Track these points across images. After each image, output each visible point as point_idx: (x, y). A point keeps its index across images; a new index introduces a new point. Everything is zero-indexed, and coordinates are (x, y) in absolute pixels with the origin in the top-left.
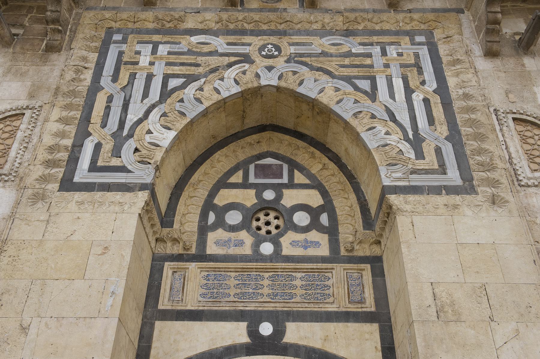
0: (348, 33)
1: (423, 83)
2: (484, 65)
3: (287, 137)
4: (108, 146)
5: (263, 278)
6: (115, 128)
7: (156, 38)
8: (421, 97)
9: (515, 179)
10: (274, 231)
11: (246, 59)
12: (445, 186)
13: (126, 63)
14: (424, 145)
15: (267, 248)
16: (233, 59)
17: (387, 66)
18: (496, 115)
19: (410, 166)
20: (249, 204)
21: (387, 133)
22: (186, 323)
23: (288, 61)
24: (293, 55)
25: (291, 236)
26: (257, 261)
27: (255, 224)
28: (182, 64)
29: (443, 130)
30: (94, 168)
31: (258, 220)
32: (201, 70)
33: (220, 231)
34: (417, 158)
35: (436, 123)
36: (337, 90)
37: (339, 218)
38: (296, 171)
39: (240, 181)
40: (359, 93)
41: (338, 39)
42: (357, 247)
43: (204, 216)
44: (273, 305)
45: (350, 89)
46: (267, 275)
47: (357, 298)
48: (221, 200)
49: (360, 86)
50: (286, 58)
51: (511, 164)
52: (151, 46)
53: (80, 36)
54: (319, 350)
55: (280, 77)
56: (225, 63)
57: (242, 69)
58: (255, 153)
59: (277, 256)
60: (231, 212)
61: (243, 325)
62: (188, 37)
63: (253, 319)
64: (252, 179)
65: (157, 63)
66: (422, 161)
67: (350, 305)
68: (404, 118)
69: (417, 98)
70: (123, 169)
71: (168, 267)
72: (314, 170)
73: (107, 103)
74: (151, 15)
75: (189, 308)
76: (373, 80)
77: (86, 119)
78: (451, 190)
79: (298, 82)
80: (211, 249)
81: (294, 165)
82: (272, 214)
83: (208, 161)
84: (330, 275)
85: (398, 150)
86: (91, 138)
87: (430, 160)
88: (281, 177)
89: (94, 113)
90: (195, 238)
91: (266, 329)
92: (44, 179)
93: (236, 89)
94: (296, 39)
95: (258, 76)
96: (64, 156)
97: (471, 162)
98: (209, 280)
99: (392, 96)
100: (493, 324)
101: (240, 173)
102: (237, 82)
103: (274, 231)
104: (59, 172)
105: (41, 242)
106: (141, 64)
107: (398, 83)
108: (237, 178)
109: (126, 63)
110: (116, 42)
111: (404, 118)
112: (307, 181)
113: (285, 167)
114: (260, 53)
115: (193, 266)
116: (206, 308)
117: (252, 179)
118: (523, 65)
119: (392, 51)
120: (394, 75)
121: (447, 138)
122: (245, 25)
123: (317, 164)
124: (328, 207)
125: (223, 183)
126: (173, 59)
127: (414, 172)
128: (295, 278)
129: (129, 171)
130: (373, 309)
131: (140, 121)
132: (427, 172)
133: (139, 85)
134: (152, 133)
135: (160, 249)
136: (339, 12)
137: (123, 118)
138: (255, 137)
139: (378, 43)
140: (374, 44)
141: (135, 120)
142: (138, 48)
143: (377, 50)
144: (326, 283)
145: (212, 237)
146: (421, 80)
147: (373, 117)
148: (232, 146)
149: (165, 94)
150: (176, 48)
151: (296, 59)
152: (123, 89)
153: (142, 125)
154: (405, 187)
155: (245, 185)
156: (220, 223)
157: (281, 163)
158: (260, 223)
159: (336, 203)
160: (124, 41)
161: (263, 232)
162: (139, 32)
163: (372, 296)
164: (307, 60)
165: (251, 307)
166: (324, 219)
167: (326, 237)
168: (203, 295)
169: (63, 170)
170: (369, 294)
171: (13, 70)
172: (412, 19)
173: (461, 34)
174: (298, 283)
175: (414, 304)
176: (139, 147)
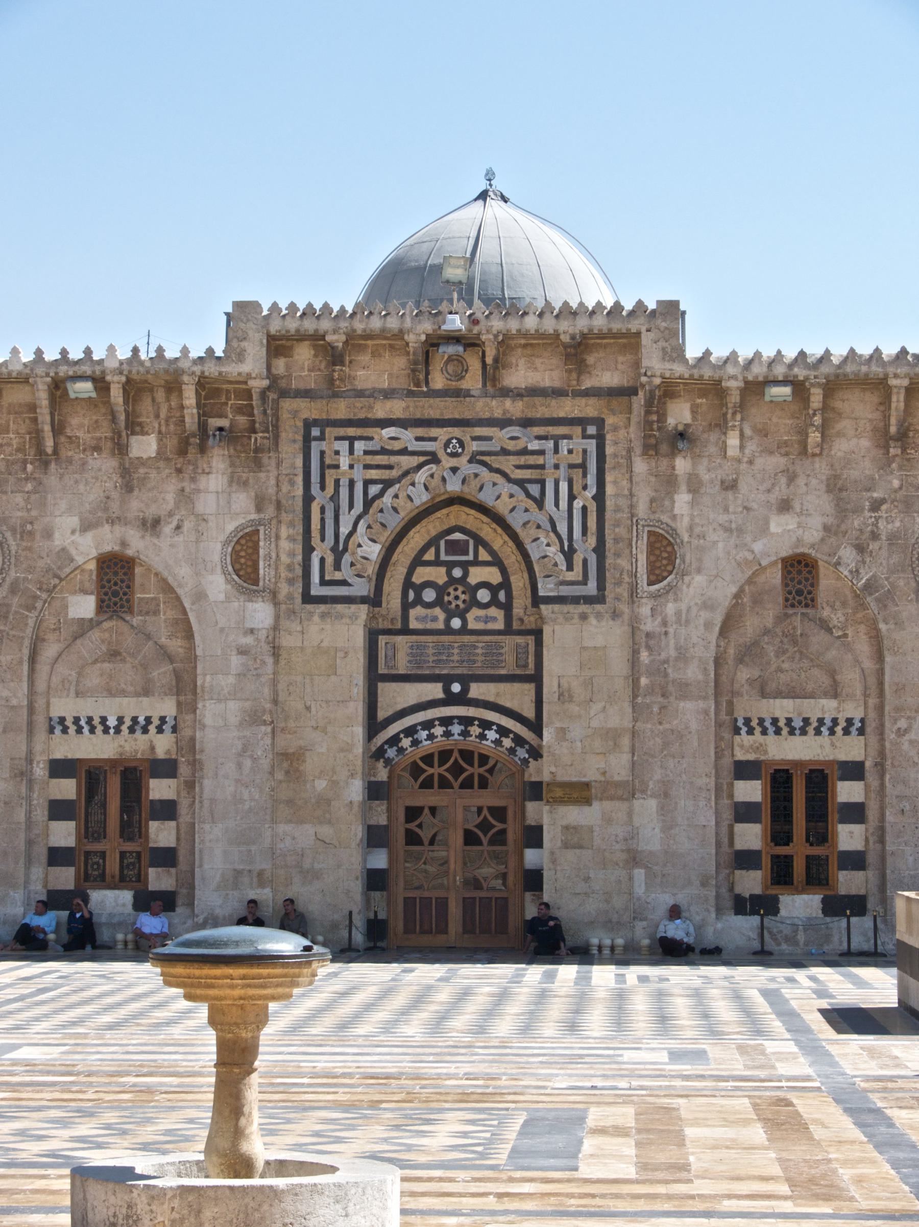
0: (526, 423)
1: (585, 487)
2: (640, 466)
3: (473, 512)
4: (330, 559)
5: (453, 648)
6: (332, 543)
7: (351, 431)
8: (581, 504)
10: (462, 606)
14: (575, 556)
15: (456, 623)
16: (422, 459)
17: (557, 467)
21: (548, 545)
23: (470, 461)
25: (475, 612)
28: (378, 467)
29: (592, 541)
30: (323, 582)
31: (449, 594)
32: (395, 473)
33: (419, 608)
36: (511, 496)
39: (433, 558)
41: (515, 431)
43: (405, 594)
45: (521, 495)
47: (522, 663)
48: (417, 579)
49: (532, 492)
52: (347, 443)
53: (283, 435)
55: (464, 481)
58: (445, 527)
59: (464, 630)
61: (439, 686)
62: (378, 429)
63: (447, 681)
64: (443, 557)
68: (562, 528)
69: (578, 504)
70: (344, 583)
71: (382, 640)
72: (497, 545)
76: (542, 483)
78: (589, 600)
81: (480, 541)
83: (405, 541)
86: (315, 553)
87: (576, 574)
88: (467, 554)
89: (313, 527)
90: (400, 613)
91: (456, 688)
94: (479, 431)
95: (444, 479)
96: (299, 571)
97: (608, 574)
99: (557, 505)
101: (433, 550)
102: (426, 488)
105: (302, 649)
107: (564, 487)
108: (429, 556)
110: (316, 439)
111: (562, 528)
112: (489, 558)
113: (471, 542)
115: (399, 639)
118: (673, 468)
119: (564, 445)
121: (594, 550)
123: (498, 540)
124: (506, 584)
126: (369, 459)
129: (350, 585)
143: (550, 444)
147: (539, 527)
149: (368, 503)
152: (331, 498)
154: (554, 597)
155: (437, 563)
156: (419, 601)
159: (513, 579)
160: (322, 438)
161: (453, 606)
164: (486, 459)
165: (445, 672)
166: (502, 596)
167: (502, 612)
168: (410, 662)
171: (235, 479)
173: (628, 426)
174: (479, 651)
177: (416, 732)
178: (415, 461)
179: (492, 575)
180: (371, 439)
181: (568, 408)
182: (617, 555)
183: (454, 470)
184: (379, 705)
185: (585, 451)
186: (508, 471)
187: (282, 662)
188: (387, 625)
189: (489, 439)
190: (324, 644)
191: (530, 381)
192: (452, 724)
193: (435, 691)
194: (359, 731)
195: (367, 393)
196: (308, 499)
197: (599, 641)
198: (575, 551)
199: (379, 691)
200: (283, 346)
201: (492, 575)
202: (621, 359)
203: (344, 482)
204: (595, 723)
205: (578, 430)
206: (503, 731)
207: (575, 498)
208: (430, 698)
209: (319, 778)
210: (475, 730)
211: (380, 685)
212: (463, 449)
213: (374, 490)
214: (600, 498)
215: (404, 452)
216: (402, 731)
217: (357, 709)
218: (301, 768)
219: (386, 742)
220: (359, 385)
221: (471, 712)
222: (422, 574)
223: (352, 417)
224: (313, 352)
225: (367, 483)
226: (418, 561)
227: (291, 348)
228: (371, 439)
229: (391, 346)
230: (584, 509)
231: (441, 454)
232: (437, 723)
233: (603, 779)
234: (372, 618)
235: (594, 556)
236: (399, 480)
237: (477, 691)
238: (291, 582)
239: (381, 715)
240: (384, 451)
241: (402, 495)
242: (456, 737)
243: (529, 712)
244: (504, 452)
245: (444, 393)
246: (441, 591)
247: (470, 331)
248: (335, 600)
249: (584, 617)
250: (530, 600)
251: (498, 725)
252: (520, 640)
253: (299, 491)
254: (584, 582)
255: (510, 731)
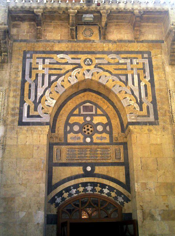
0: (118, 53)
1: (145, 77)
4: (32, 107)
7: (44, 55)
8: (144, 84)
9: (172, 120)
10: (90, 133)
11: (79, 66)
12: (149, 122)
13: (34, 69)
14: (143, 105)
15: (88, 140)
16: (74, 66)
18: (170, 92)
19: (138, 114)
20: (81, 123)
21: (131, 100)
22: (63, 167)
23: (95, 67)
24: (97, 64)
26: (85, 145)
27: (84, 130)
28: (55, 69)
29: (150, 99)
30: (28, 116)
31: (85, 128)
32: (62, 72)
33: (72, 133)
34: (140, 111)
35: (148, 95)
36: (113, 81)
37: (113, 127)
38: (98, 109)
40: (121, 83)
41: (114, 56)
42: (119, 139)
43: (65, 128)
44: (90, 160)
45: (118, 80)
46: (88, 150)
48: (71, 122)
50: (94, 66)
51: (172, 113)
52: (42, 60)
54: (106, 175)
55: (92, 75)
56: (71, 68)
57: (78, 71)
59: (92, 143)
60: (75, 126)
61: (81, 167)
62: (56, 55)
63: (85, 165)
64: (82, 112)
65: (45, 68)
66: (142, 112)
67: (116, 160)
68: (137, 93)
69: (142, 84)
70: (39, 116)
72: (105, 108)
73: (29, 87)
74: (40, 45)
75: (63, 162)
77: (22, 95)
78: (151, 123)
79: (99, 77)
80: (69, 141)
81: (97, 106)
82: (90, 126)
83: (66, 105)
84: (109, 149)
85: (134, 107)
86: (25, 104)
91: (89, 169)
92: (13, 121)
93: (76, 81)
94: (98, 56)
95: (84, 74)
96: (17, 111)
97: (159, 112)
98: (69, 152)
100: (158, 170)
101: (78, 110)
102: (76, 78)
103: (90, 133)
104: (17, 117)
106: (39, 69)
107: (136, 77)
109: (34, 69)
110: (28, 58)
111: (137, 93)
112: (102, 113)
113: (94, 107)
114: (84, 63)
115: (63, 147)
116: (69, 162)
117: (82, 112)
119: (135, 61)
120: (135, 74)
121: (151, 102)
122: (78, 49)
123: (106, 106)
124: (109, 123)
125: (71, 114)
127: (138, 116)
128: (98, 151)
130: (123, 161)
131: (42, 96)
132: (143, 116)
133: (40, 79)
134: (47, 101)
135: (51, 141)
136: (115, 42)
137: (36, 94)
138: (83, 94)
139: (129, 58)
140: (128, 58)
141: (40, 95)
142: (37, 61)
143: (129, 61)
144: (108, 152)
145: (69, 136)
146: (145, 75)
147: (126, 93)
148: (74, 98)
149: (50, 84)
150: (52, 61)
151: (98, 66)
152: (34, 81)
153: (43, 98)
154: (135, 122)
155: (79, 115)
156: (72, 131)
157: (92, 105)
158: (85, 130)
160: (31, 57)
162: (36, 52)
163: (123, 157)
165: (84, 161)
167: (108, 135)
169: (18, 117)
170: (122, 155)
172: (143, 46)
174: (99, 152)
175: (135, 165)
176: (43, 107)
177: (71, 190)
178: (71, 67)
179: (104, 120)
180: (53, 58)
181: (137, 47)
182: (163, 103)
183: (88, 71)
184: (53, 177)
185: (144, 64)
186: (112, 71)
187: (6, 152)
188: (57, 141)
189: (103, 58)
190: (27, 143)
191: (119, 37)
192: (87, 186)
193: (78, 170)
194: (43, 186)
195: (52, 41)
196: (24, 81)
197: (159, 141)
198: (143, 103)
199: (53, 170)
200: (17, 24)
201: (104, 120)
202: (155, 30)
203: (40, 75)
204: (159, 181)
205: (141, 55)
206: (111, 189)
207: (141, 81)
208: (77, 173)
209: (22, 211)
210: (98, 189)
211: (54, 168)
212: (92, 63)
213: (53, 78)
214: (152, 81)
215: (67, 63)
216: (64, 189)
217: (43, 175)
218: (12, 206)
219: (56, 195)
220: (47, 38)
221: (96, 180)
222: (73, 120)
223: (44, 50)
224: (29, 26)
225: (50, 75)
226: (71, 114)
227: (20, 24)
228: (53, 58)
229: (61, 25)
230: (145, 86)
231: (82, 64)
232: (80, 185)
233: (167, 209)
234: (50, 137)
235: (152, 105)
236: (64, 74)
237: (98, 170)
238: (13, 115)
239: (54, 181)
240: (58, 63)
241: (66, 80)
242: (89, 192)
243: (123, 179)
244: (109, 63)
245: (85, 41)
246: (82, 127)
247: (96, 8)
248: (34, 124)
249: (150, 131)
250: (120, 129)
251: (109, 186)
252: (116, 147)
253: (20, 79)
254: (148, 116)
255: (115, 189)
